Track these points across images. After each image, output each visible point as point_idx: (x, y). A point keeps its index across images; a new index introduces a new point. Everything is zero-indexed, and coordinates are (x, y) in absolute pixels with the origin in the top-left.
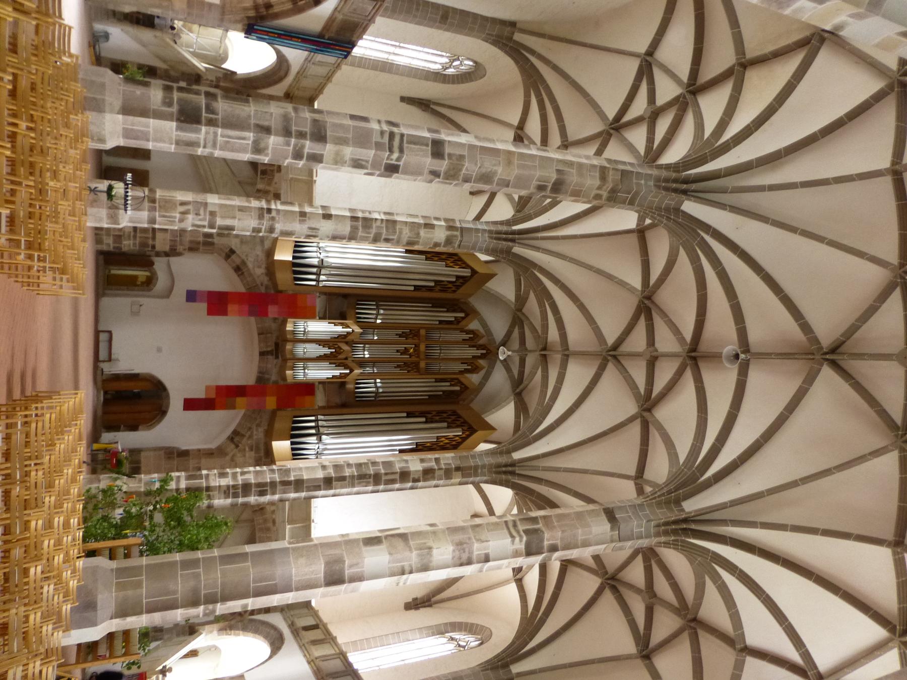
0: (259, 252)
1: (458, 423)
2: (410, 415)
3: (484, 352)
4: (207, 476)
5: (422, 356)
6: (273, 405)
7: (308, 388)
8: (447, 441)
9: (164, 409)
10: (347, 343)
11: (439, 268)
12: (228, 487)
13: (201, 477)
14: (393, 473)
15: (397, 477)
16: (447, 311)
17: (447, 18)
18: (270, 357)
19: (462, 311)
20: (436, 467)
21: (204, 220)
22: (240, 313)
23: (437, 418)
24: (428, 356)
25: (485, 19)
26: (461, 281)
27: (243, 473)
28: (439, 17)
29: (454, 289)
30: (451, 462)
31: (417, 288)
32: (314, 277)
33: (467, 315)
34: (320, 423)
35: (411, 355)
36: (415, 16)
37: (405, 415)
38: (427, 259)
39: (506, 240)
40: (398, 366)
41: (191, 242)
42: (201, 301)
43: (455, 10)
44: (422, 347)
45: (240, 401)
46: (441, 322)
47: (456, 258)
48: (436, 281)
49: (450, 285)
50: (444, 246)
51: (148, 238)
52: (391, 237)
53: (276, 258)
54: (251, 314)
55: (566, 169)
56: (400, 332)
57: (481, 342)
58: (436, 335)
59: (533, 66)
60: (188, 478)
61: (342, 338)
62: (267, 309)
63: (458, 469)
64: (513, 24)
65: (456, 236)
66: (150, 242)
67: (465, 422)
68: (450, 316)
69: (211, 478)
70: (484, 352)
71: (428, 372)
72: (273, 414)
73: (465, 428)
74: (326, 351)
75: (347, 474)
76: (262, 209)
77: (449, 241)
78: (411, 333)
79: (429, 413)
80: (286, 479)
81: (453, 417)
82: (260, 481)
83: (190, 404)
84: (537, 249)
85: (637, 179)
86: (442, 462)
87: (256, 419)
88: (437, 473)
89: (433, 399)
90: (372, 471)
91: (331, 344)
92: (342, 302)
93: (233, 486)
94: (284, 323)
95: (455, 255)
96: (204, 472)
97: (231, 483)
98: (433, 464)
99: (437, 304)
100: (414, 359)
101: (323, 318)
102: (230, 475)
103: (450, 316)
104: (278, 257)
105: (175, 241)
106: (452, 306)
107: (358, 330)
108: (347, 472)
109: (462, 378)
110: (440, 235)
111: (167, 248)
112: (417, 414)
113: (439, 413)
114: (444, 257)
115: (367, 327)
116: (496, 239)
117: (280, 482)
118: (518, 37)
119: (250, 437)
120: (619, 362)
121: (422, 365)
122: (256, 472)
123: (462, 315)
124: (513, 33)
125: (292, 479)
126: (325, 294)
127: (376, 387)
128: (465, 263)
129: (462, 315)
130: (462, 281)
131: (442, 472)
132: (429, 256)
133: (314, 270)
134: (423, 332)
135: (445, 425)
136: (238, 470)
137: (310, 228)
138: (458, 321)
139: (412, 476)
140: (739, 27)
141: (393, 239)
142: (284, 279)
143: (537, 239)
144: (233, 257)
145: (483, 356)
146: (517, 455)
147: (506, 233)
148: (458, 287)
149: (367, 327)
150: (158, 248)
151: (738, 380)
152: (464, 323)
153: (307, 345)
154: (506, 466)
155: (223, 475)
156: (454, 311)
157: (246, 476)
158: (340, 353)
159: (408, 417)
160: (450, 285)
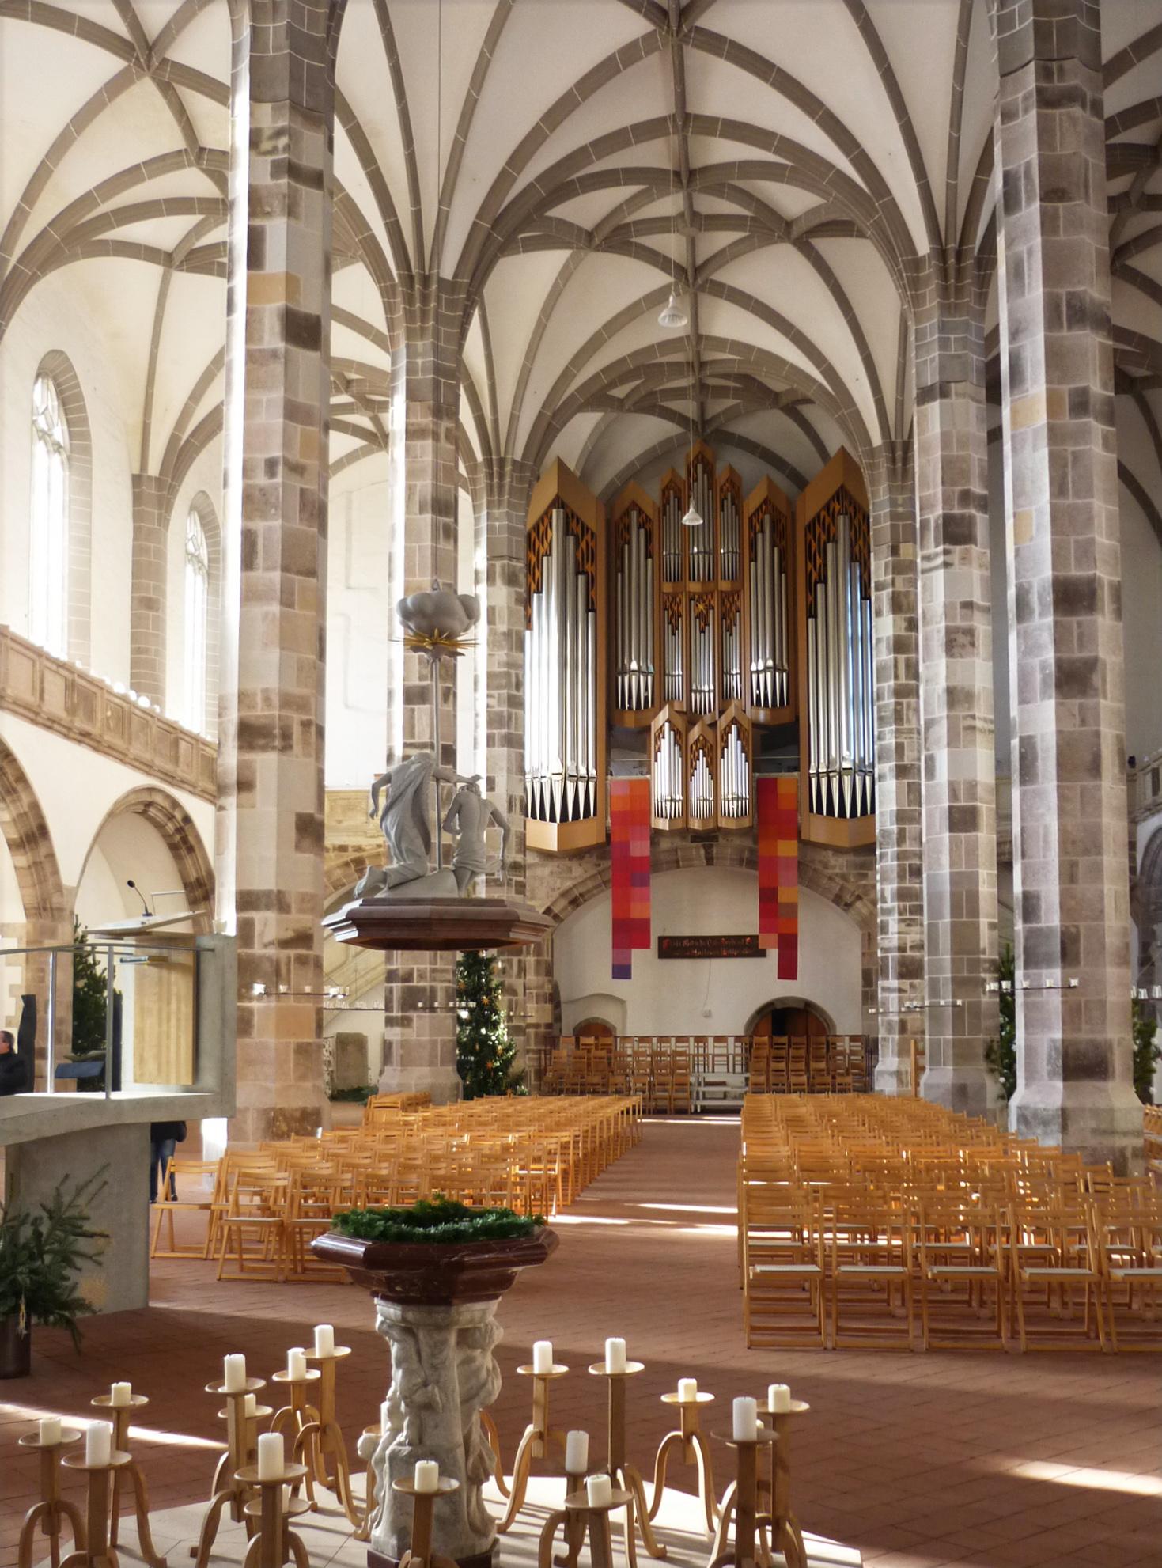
0: (545, 871)
1: (828, 520)
2: (812, 613)
3: (700, 467)
4: (885, 950)
6: (793, 837)
7: (762, 791)
9: (801, 1006)
10: (688, 731)
11: (551, 568)
12: (901, 921)
13: (885, 959)
14: (896, 666)
15: (902, 658)
16: (629, 543)
17: (150, 599)
18: (715, 850)
19: (627, 513)
20: (890, 590)
21: (510, 962)
22: (646, 899)
23: (819, 561)
24: (711, 577)
25: (137, 531)
26: (573, 525)
27: (884, 900)
28: (151, 613)
29: (588, 537)
30: (883, 562)
31: (590, 607)
32: (582, 786)
34: (823, 769)
35: (710, 607)
36: (157, 653)
37: (811, 621)
38: (539, 591)
39: (501, 476)
40: (729, 630)
41: (537, 973)
42: (629, 958)
43: (135, 588)
44: (695, 587)
45: (784, 895)
46: (649, 554)
47: (534, 535)
48: (577, 573)
49: (583, 545)
50: (520, 586)
51: (536, 1034)
52: (514, 680)
53: (554, 848)
54: (645, 883)
55: (417, 499)
56: (669, 629)
57: (683, 473)
58: (671, 562)
59: (193, 434)
60: (887, 978)
61: (680, 738)
62: (635, 859)
63: (895, 551)
64: (137, 480)
65: (503, 567)
66: (542, 1030)
67: (827, 507)
69: (886, 944)
70: (700, 467)
71: (737, 576)
72: (805, 844)
73: (838, 507)
74: (701, 763)
75: (893, 741)
76: (487, 882)
77: (511, 580)
78: (668, 614)
79: (809, 576)
80: (895, 837)
81: (818, 530)
82: (895, 874)
83: (787, 970)
84: (514, 419)
85: (416, 373)
86: (882, 578)
87: (815, 870)
88: (900, 587)
89: (785, 565)
90: (889, 701)
91: (691, 756)
92: (621, 733)
93: (900, 914)
94: (658, 833)
95: (529, 536)
96: (879, 954)
97: (896, 916)
98: (885, 595)
99: (616, 564)
100: (715, 602)
101: (646, 767)
102: (885, 918)
103: (637, 538)
104: (553, 847)
105: (537, 995)
106: (617, 535)
107: (664, 715)
108: (890, 741)
109: (751, 504)
110: (503, 595)
111: (549, 1006)
112: (811, 598)
113: (810, 556)
114: (534, 559)
115: (662, 696)
116: (501, 493)
117: (899, 845)
118: (153, 469)
119: (844, 877)
120: (706, 263)
121: (725, 586)
122: (883, 880)
123: (634, 514)
124: (150, 478)
125: (895, 827)
126: (608, 764)
127: (766, 669)
128: (542, 519)
129: (634, 514)
130: (573, 526)
131: (899, 579)
132: (533, 587)
133: (570, 787)
134: (667, 588)
135: (830, 546)
136: (879, 906)
137: (510, 809)
139: (903, 633)
140: (137, 167)
141: (517, 676)
142: (589, 834)
143: (496, 421)
144: (556, 910)
145: (709, 470)
146: (877, 440)
147: (490, 476)
148: (585, 529)
149: (662, 696)
150: (548, 1019)
151: (723, 135)
152: (649, 511)
153: (693, 798)
154: (894, 461)
155: (884, 928)
156: (628, 529)
157: (888, 895)
158: (705, 740)
159: (815, 617)
160: (583, 545)
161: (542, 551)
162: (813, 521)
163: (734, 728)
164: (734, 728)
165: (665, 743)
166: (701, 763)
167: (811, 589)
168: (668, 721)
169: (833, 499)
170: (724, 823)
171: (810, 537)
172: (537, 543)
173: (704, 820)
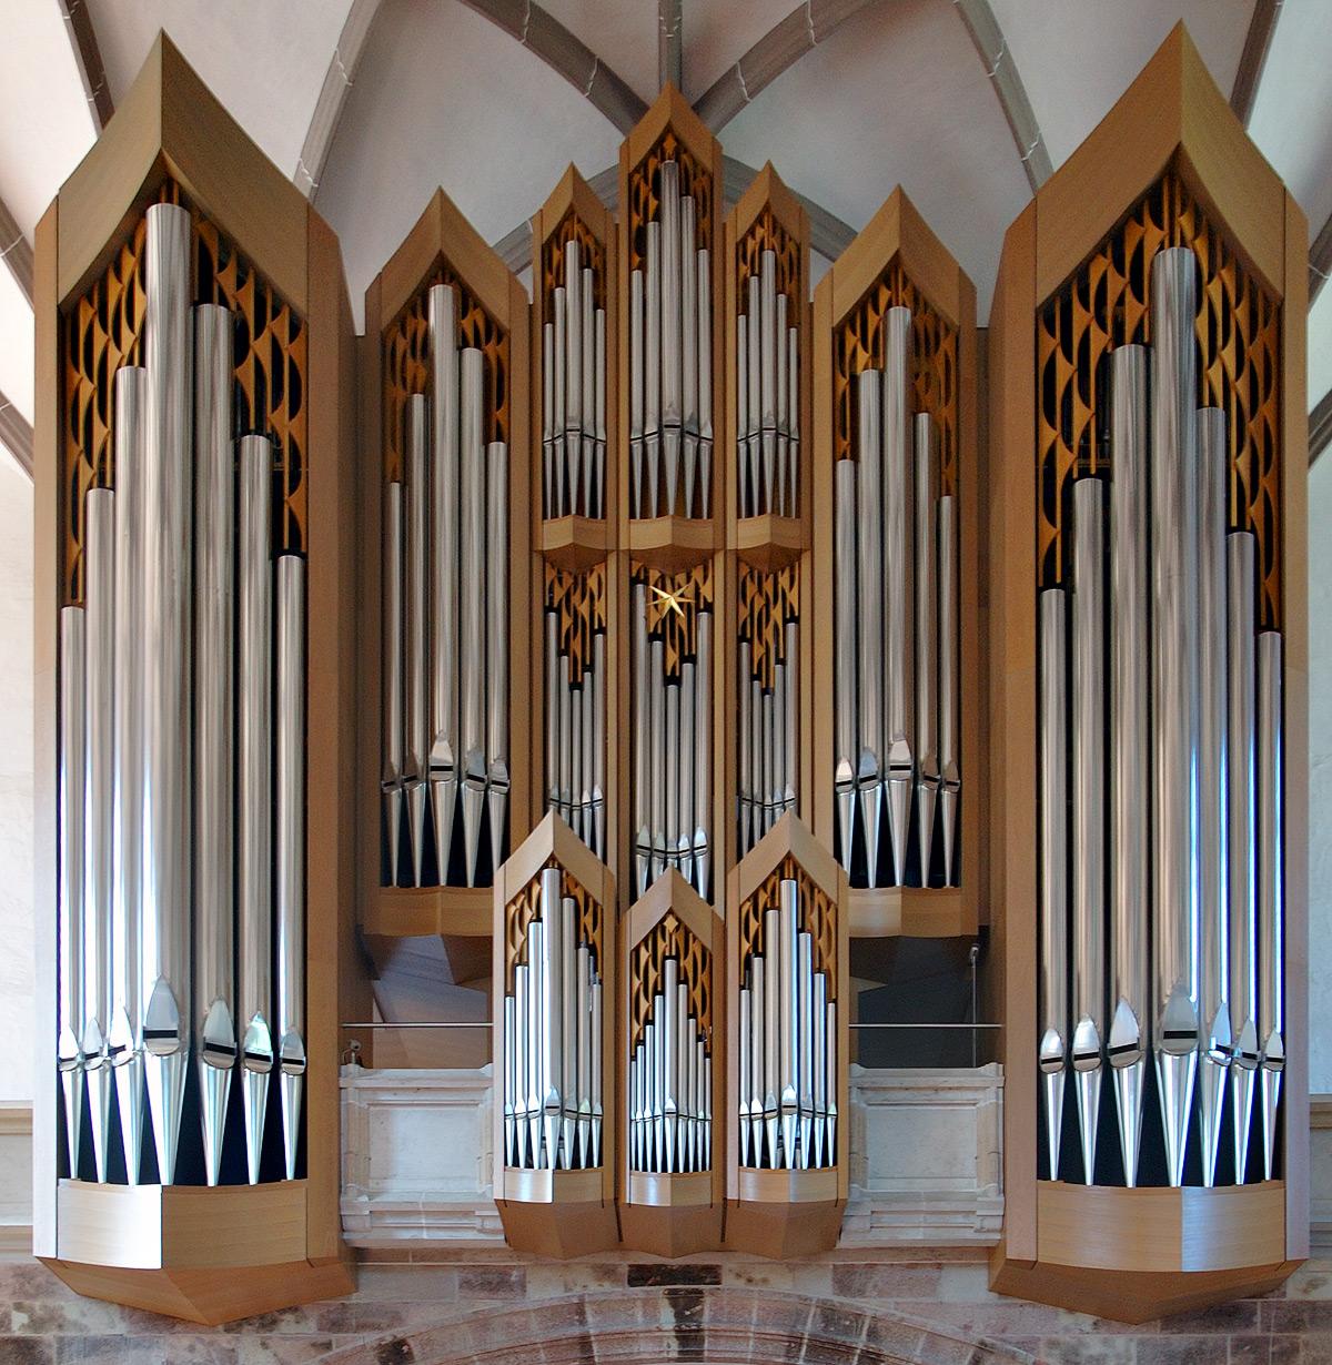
5: (702, 535)
8: (1228, 355)
16: (428, 392)
19: (419, 304)
23: (1082, 415)
33: (443, 270)
44: (651, 534)
46: (493, 431)
67: (1114, 241)
68: (456, 377)
81: (1081, 318)
99: (384, 444)
103: (456, 377)
112: (1052, 532)
113: (1049, 404)
121: (751, 533)
123: (440, 300)
129: (440, 300)
134: (557, 534)
138: (479, 329)
156: (423, 349)
161: (114, 356)
162: (1063, 293)
163: (788, 890)
164: (788, 890)
165: (541, 938)
166: (669, 1008)
167: (1053, 500)
168: (552, 861)
169: (1134, 214)
170: (746, 1186)
171: (1051, 343)
172: (100, 339)
173: (681, 1171)
